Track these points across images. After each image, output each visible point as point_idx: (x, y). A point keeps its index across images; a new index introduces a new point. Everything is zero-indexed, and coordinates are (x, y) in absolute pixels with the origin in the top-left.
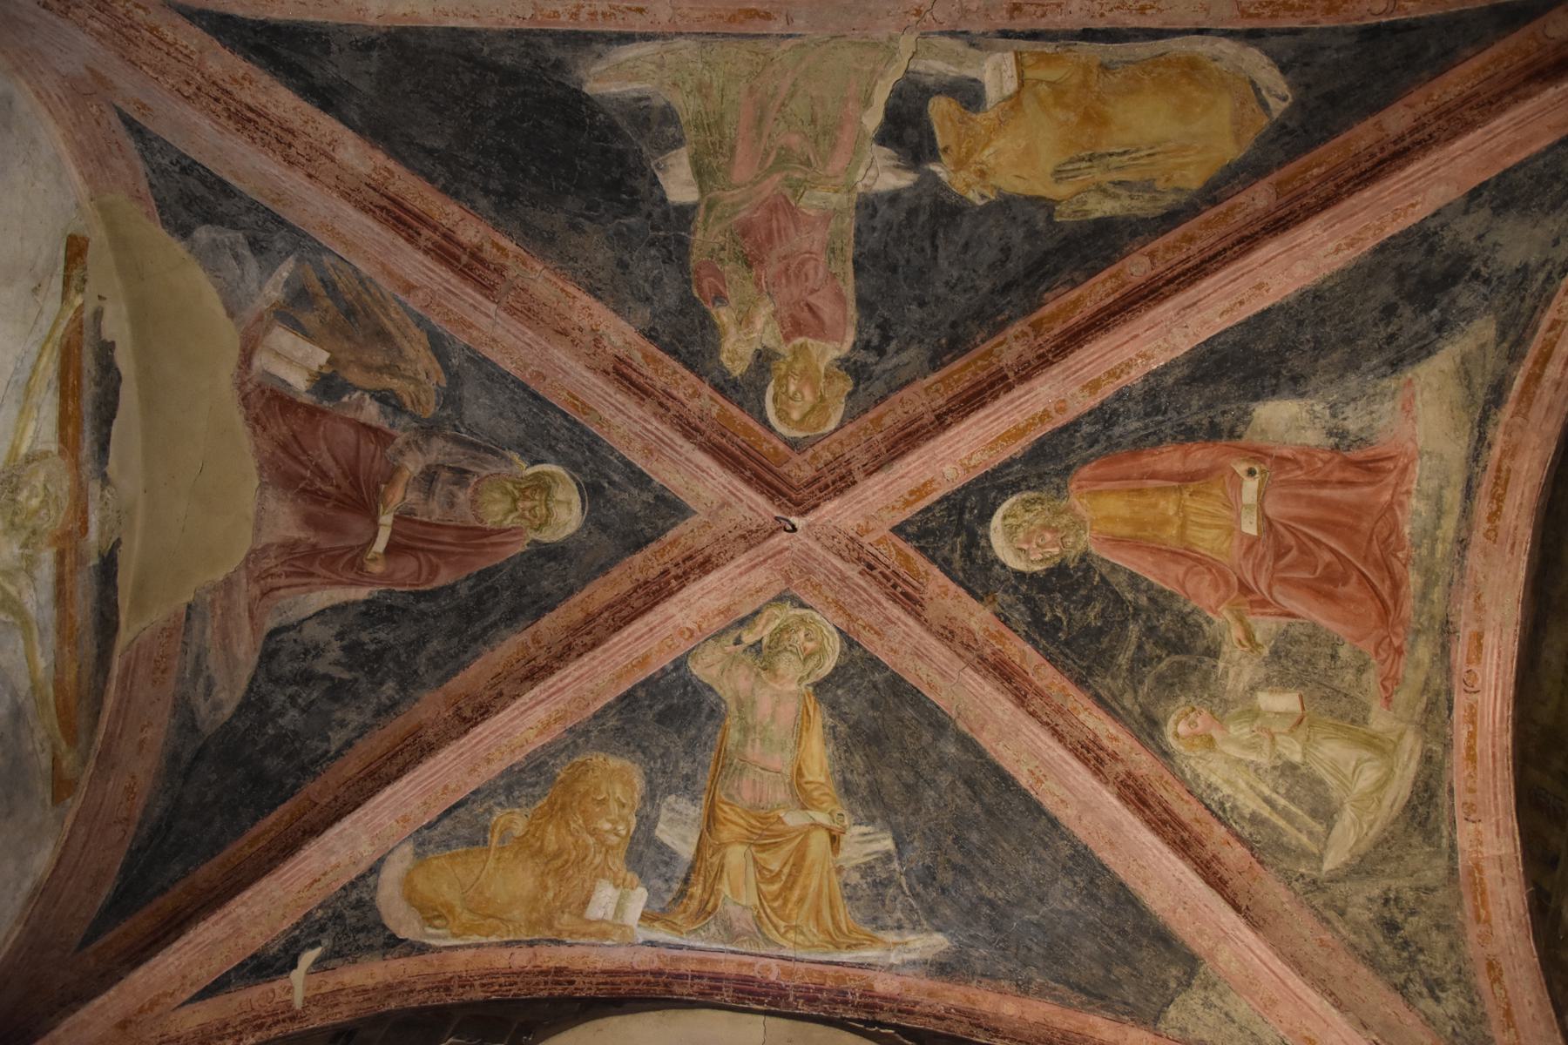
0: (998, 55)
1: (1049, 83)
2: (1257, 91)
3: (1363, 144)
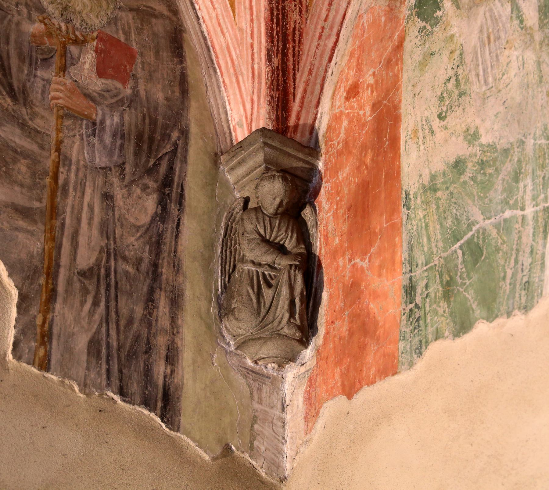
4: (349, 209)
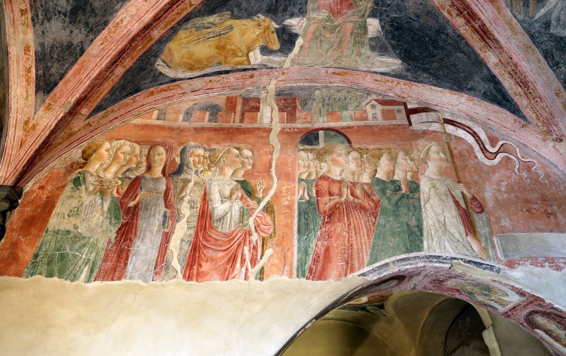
0: (256, 63)
1: (238, 56)
2: (167, 65)
3: (127, 60)
4: (25, 220)
